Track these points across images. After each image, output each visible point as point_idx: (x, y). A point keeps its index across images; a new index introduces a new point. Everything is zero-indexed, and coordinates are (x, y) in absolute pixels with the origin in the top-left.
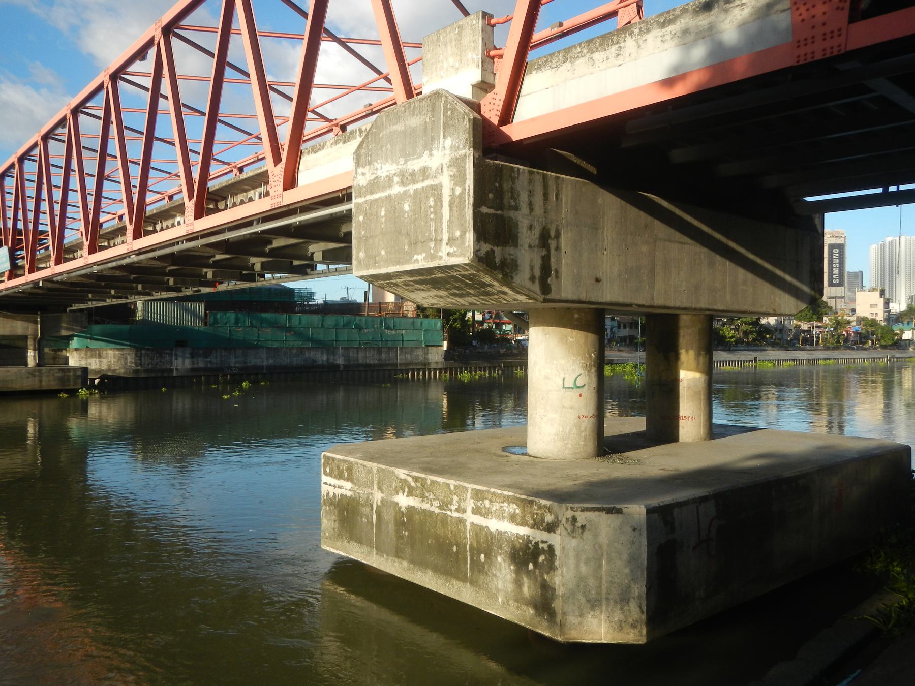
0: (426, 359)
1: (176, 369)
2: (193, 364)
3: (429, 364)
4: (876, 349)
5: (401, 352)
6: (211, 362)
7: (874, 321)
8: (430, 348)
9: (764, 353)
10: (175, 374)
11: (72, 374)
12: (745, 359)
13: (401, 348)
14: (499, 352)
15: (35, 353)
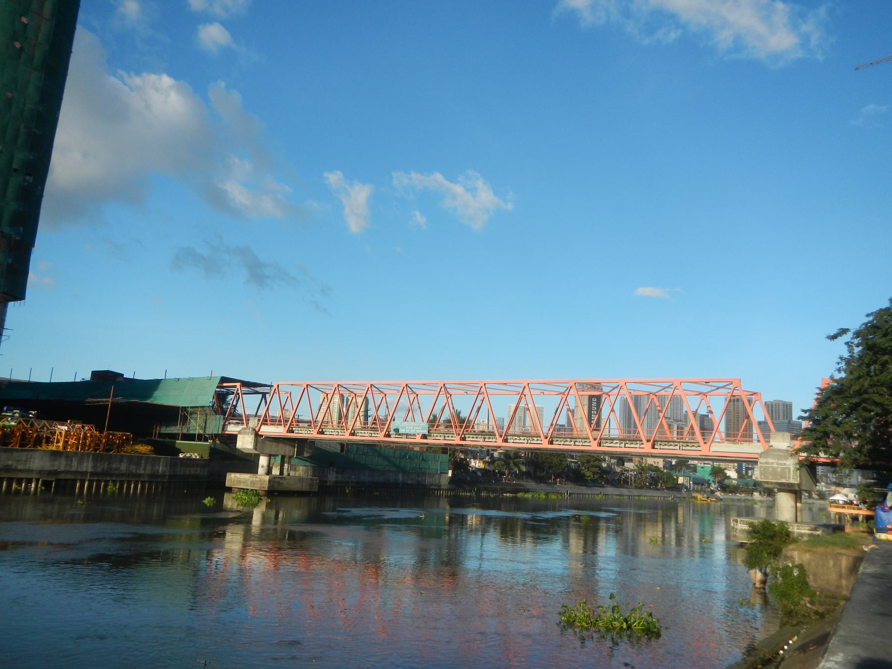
0: (439, 482)
1: (329, 481)
2: (337, 477)
3: (441, 485)
4: (663, 490)
5: (428, 475)
6: (344, 477)
7: (657, 467)
8: (442, 474)
9: (604, 489)
10: (328, 484)
11: (315, 482)
12: (596, 493)
13: (428, 473)
14: (466, 479)
15: (288, 467)
